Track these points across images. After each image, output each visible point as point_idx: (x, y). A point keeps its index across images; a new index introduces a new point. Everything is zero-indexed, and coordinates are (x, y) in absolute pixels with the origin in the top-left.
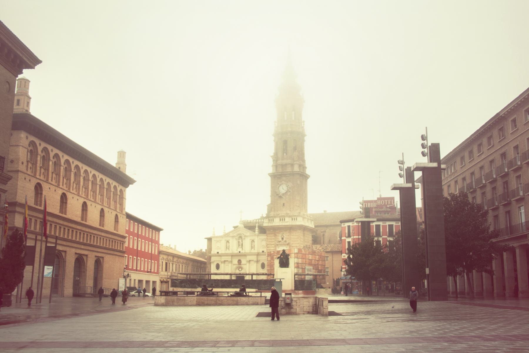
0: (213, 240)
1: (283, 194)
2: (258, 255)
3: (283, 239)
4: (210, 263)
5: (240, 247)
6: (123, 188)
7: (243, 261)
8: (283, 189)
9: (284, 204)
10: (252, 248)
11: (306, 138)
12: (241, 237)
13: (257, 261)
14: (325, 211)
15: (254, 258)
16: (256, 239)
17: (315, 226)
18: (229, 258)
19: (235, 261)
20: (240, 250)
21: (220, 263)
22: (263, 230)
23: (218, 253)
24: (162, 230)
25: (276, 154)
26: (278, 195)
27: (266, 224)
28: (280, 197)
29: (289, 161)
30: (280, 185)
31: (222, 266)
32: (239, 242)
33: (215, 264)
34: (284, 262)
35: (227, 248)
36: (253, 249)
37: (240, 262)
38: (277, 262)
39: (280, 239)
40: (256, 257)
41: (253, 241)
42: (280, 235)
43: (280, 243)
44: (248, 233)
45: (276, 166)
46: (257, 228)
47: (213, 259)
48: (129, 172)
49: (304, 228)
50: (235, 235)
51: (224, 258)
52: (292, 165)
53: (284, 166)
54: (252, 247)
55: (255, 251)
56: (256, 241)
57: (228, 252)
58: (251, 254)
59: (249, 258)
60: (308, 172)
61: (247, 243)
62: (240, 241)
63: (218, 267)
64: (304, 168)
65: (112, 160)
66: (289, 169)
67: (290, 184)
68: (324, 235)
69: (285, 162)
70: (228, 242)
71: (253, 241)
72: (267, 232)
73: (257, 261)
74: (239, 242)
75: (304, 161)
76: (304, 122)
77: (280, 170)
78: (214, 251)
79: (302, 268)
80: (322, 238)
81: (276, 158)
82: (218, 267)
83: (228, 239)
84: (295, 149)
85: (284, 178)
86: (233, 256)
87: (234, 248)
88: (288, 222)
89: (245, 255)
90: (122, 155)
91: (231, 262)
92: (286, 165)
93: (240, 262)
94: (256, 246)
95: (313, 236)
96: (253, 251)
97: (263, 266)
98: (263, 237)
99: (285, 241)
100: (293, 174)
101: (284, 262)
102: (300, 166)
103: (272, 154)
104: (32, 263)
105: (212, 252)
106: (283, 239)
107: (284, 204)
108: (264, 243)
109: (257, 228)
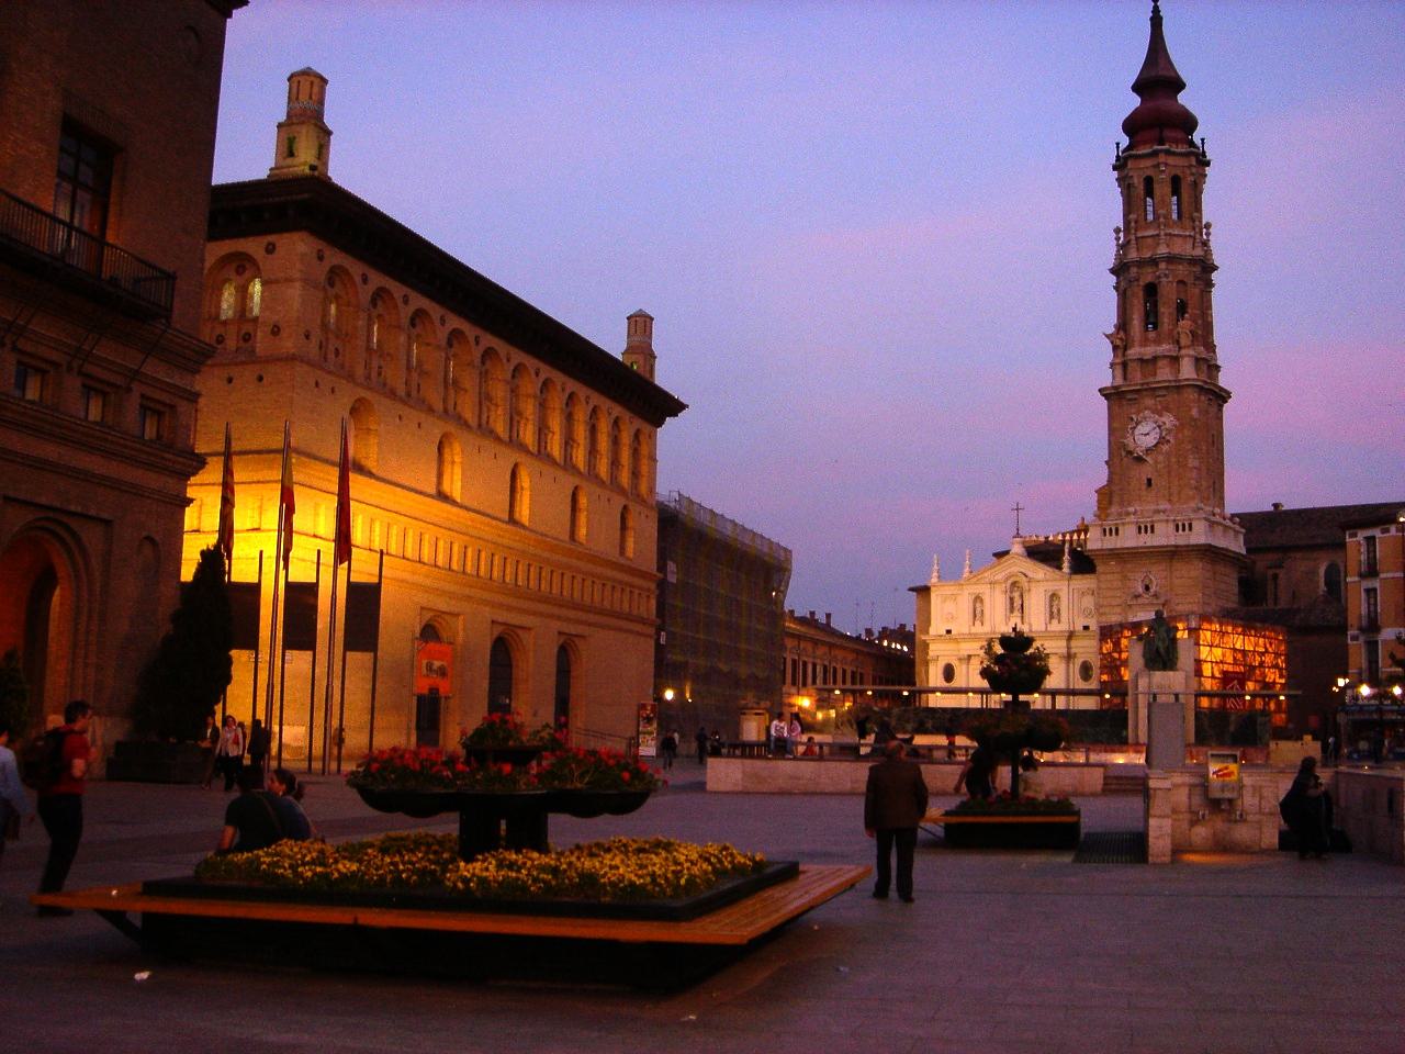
0: (933, 595)
1: (1148, 450)
3: (1147, 588)
4: (927, 663)
5: (1017, 613)
6: (646, 428)
8: (1145, 435)
9: (1149, 481)
10: (1052, 617)
11: (1214, 276)
13: (1069, 657)
14: (1276, 506)
17: (1248, 550)
21: (955, 663)
22: (1084, 563)
23: (949, 632)
25: (1123, 325)
26: (1130, 453)
27: (1094, 541)
28: (1139, 459)
29: (1165, 348)
30: (1137, 424)
32: (1012, 599)
33: (942, 664)
35: (976, 615)
36: (1055, 621)
39: (1141, 590)
40: (1064, 643)
42: (1139, 576)
43: (1140, 601)
44: (1039, 571)
45: (1122, 364)
46: (1066, 557)
47: (934, 649)
48: (665, 378)
50: (999, 577)
52: (1175, 360)
53: (1150, 363)
54: (1053, 615)
56: (1064, 595)
60: (1224, 380)
61: (1036, 603)
62: (1016, 595)
63: (949, 673)
64: (1214, 368)
65: (612, 341)
66: (1164, 374)
67: (1168, 420)
68: (1275, 577)
69: (1149, 351)
70: (978, 599)
71: (1054, 597)
72: (1100, 568)
74: (1012, 599)
75: (1211, 347)
76: (1208, 226)
77: (1137, 377)
80: (1270, 587)
81: (1121, 339)
82: (949, 673)
84: (1182, 309)
85: (1149, 402)
90: (640, 324)
92: (1155, 359)
95: (1241, 582)
96: (1055, 626)
97: (1086, 670)
98: (1084, 582)
99: (1156, 595)
100: (1179, 388)
102: (1197, 360)
103: (1111, 330)
104: (251, 643)
105: (933, 631)
106: (1147, 588)
107: (1149, 481)
108: (1089, 602)
109: (1066, 557)
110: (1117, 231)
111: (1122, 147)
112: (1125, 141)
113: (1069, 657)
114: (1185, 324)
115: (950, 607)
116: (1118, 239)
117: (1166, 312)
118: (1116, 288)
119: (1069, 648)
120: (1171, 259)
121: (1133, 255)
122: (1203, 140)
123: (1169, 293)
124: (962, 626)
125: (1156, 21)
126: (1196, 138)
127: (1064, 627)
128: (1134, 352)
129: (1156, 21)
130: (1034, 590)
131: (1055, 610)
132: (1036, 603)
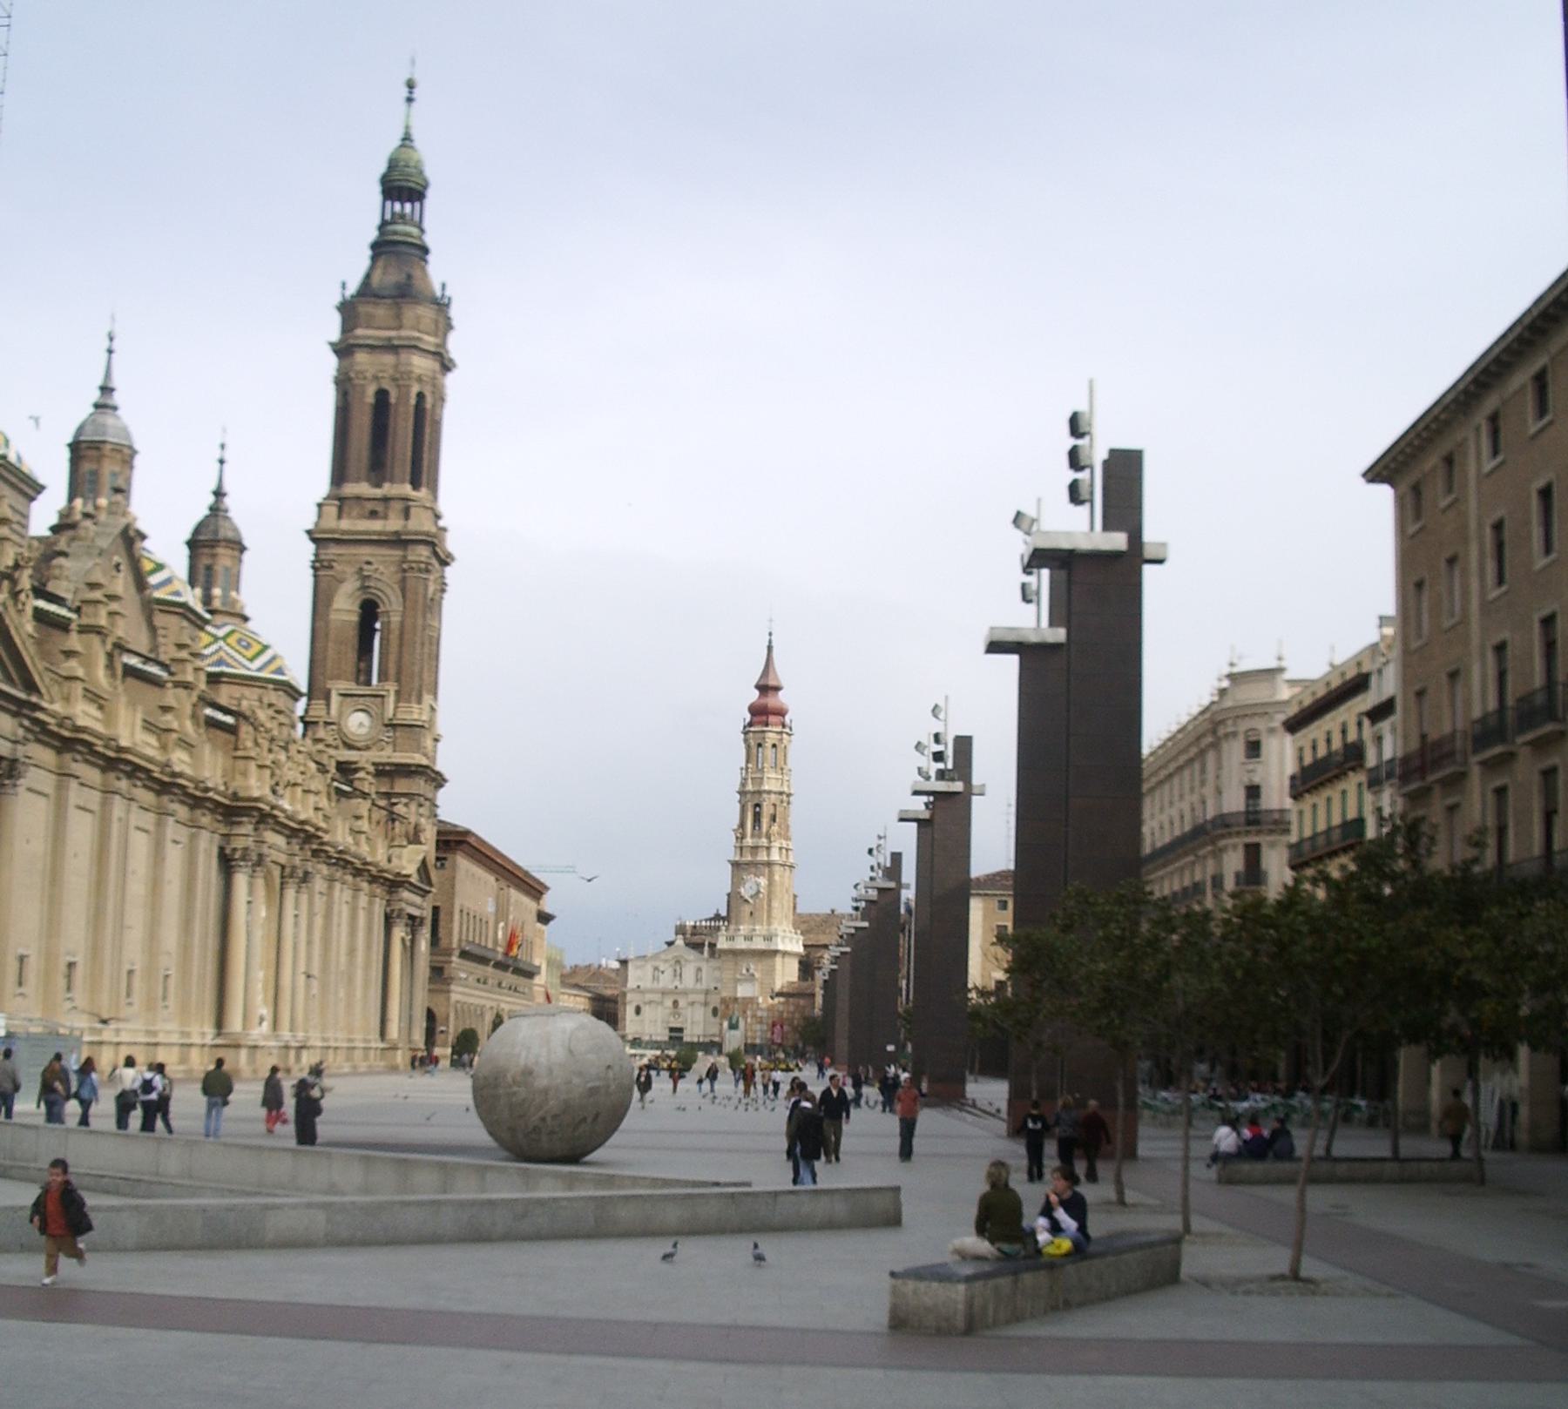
0: (630, 965)
2: (707, 992)
7: (682, 1003)
12: (678, 962)
13: (706, 1004)
15: (701, 998)
16: (704, 966)
17: (805, 946)
18: (657, 997)
19: (669, 1003)
20: (677, 983)
25: (742, 825)
27: (722, 944)
31: (645, 1010)
37: (675, 1003)
38: (726, 1024)
41: (699, 970)
44: (691, 955)
47: (629, 997)
49: (785, 954)
51: (649, 997)
52: (768, 848)
53: (755, 849)
55: (703, 986)
57: (655, 985)
58: (694, 991)
59: (692, 997)
61: (689, 972)
63: (638, 1011)
66: (762, 857)
71: (699, 970)
73: (706, 1004)
78: (631, 984)
82: (638, 1011)
83: (657, 963)
84: (774, 818)
86: (664, 993)
87: (666, 981)
88: (759, 944)
89: (685, 993)
91: (661, 1003)
93: (675, 1003)
96: (699, 986)
97: (715, 1012)
98: (714, 963)
100: (769, 864)
112: (748, 717)
114: (775, 828)
115: (639, 972)
117: (765, 821)
120: (769, 792)
121: (750, 787)
123: (767, 810)
124: (647, 984)
125: (770, 648)
126: (787, 719)
128: (749, 841)
129: (770, 648)
132: (689, 972)
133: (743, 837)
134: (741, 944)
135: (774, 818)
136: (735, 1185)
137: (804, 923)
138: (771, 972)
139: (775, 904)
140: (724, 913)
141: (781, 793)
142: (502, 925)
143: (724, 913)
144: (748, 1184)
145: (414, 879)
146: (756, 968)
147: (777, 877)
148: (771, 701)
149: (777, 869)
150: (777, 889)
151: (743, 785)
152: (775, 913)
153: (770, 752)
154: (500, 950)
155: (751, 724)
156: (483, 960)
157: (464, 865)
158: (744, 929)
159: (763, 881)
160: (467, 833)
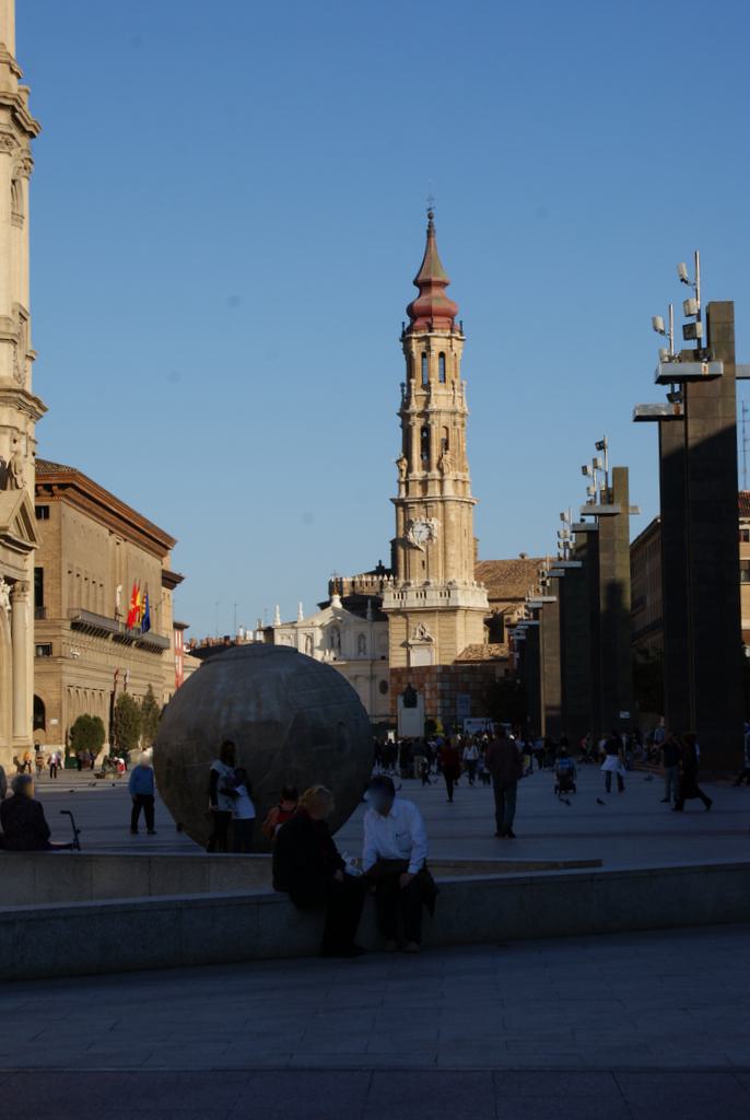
10: (360, 651)
13: (372, 678)
24: (187, 627)
32: (332, 638)
34: (411, 702)
36: (362, 653)
38: (400, 700)
40: (368, 668)
46: (369, 610)
49: (467, 610)
52: (442, 482)
62: (335, 635)
71: (362, 637)
74: (332, 638)
79: (451, 699)
84: (446, 444)
88: (435, 600)
94: (368, 648)
97: (384, 687)
101: (411, 702)
110: (403, 385)
111: (406, 326)
113: (372, 678)
116: (403, 391)
118: (402, 426)
119: (371, 671)
120: (439, 412)
122: (461, 322)
125: (429, 232)
127: (369, 657)
128: (418, 473)
130: (347, 632)
131: (362, 646)
133: (410, 469)
134: (412, 601)
135: (446, 444)
136: (579, 864)
137: (488, 574)
138: (452, 632)
139: (452, 550)
140: (388, 565)
141: (454, 413)
142: (120, 588)
143: (388, 565)
144: (597, 863)
145: (13, 533)
146: (432, 627)
147: (453, 518)
148: (437, 299)
149: (451, 506)
150: (455, 533)
151: (406, 403)
152: (454, 561)
153: (435, 363)
154: (123, 620)
155: (410, 329)
156: (100, 633)
157: (68, 514)
158: (416, 582)
159: (436, 523)
160: (74, 473)
